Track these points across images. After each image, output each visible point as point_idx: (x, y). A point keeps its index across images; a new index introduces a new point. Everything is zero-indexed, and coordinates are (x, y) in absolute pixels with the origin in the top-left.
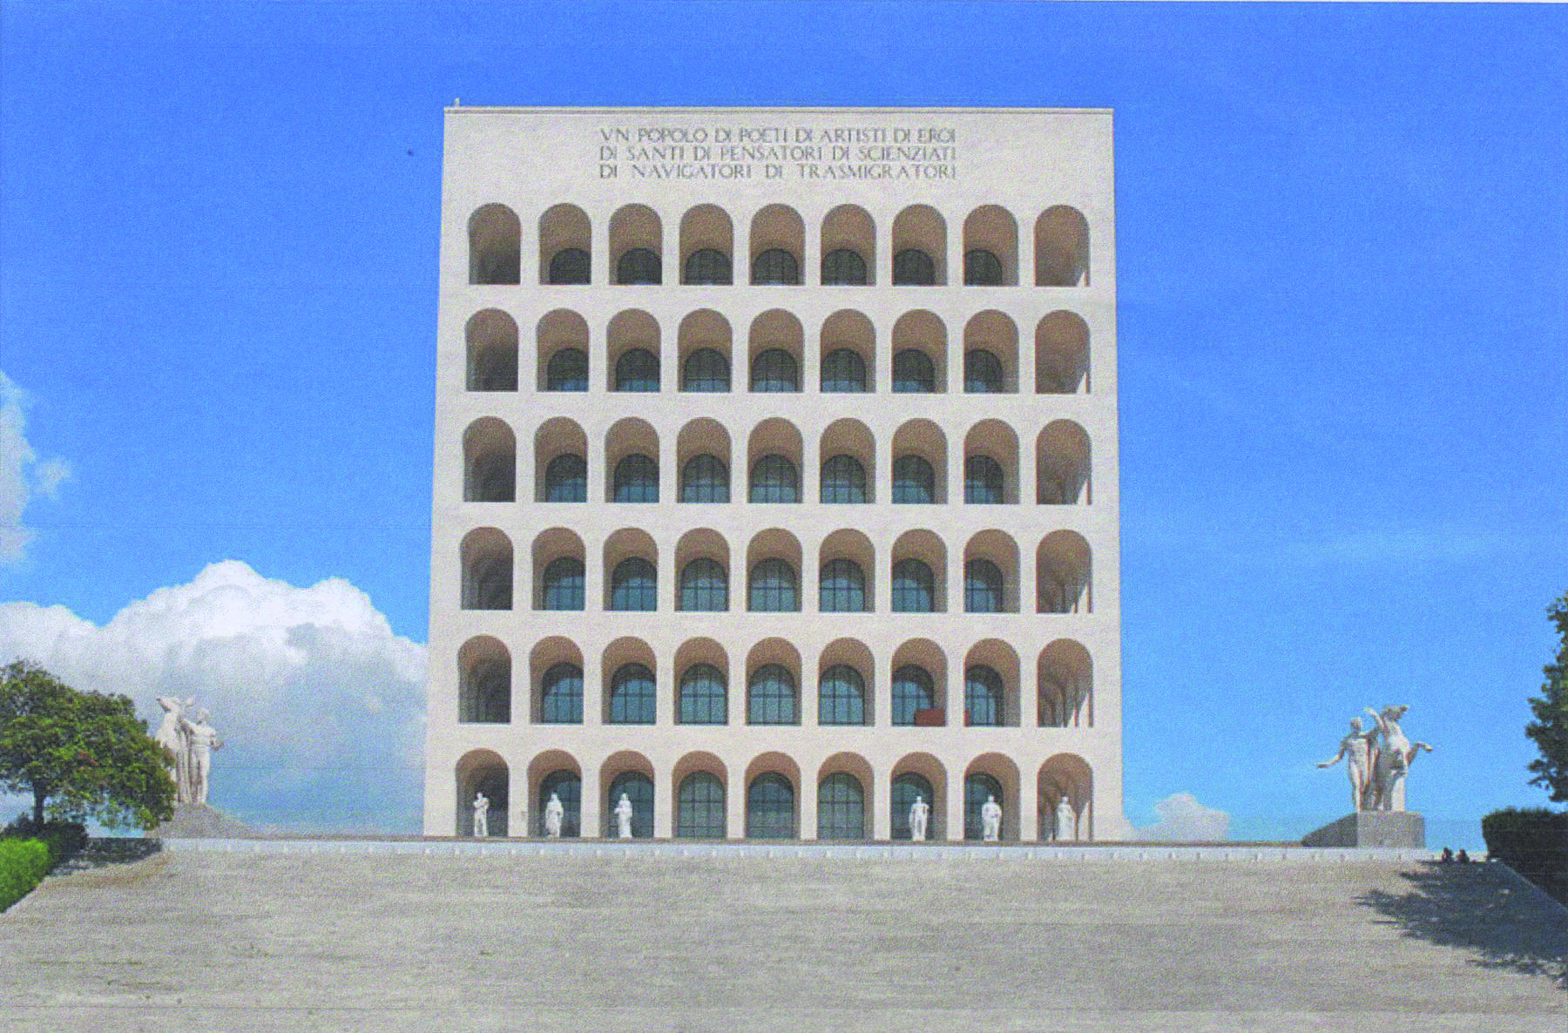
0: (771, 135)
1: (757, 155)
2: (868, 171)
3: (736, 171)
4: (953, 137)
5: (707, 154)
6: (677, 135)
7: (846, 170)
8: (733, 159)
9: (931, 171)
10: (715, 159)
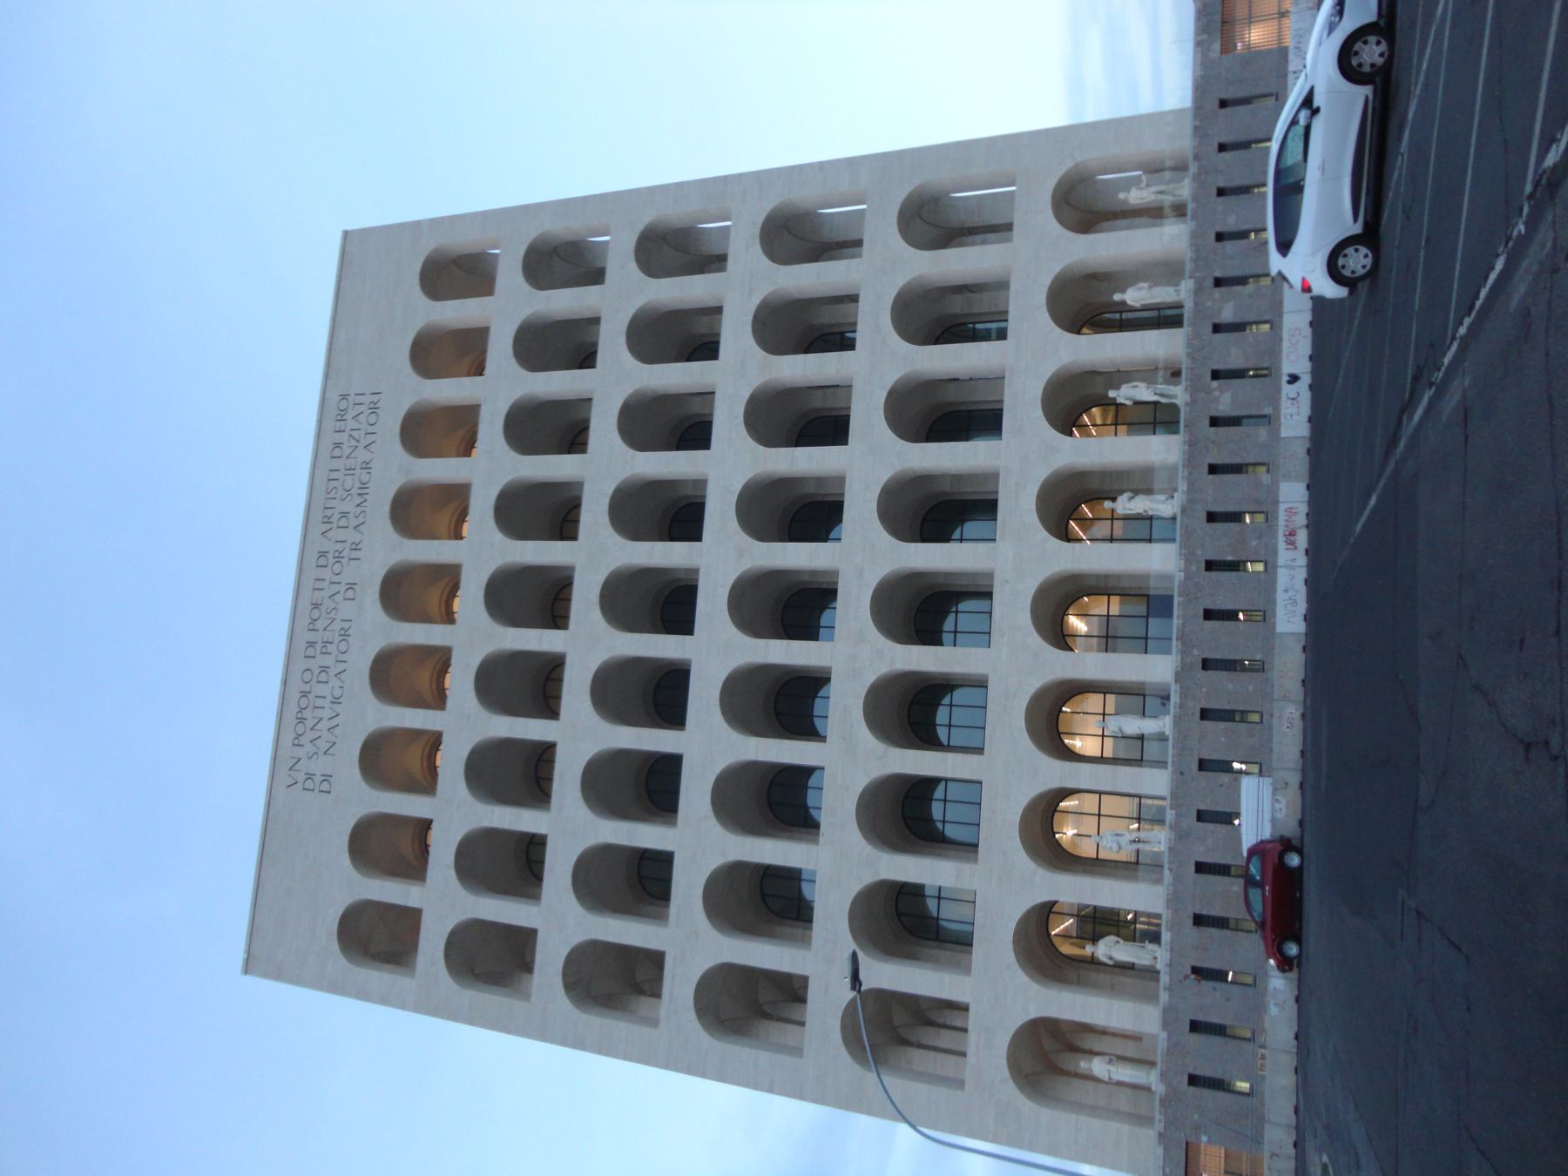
1: (332, 615)
3: (345, 635)
4: (344, 397)
5: (324, 669)
6: (304, 702)
7: (359, 510)
8: (331, 643)
9: (373, 419)
10: (328, 661)
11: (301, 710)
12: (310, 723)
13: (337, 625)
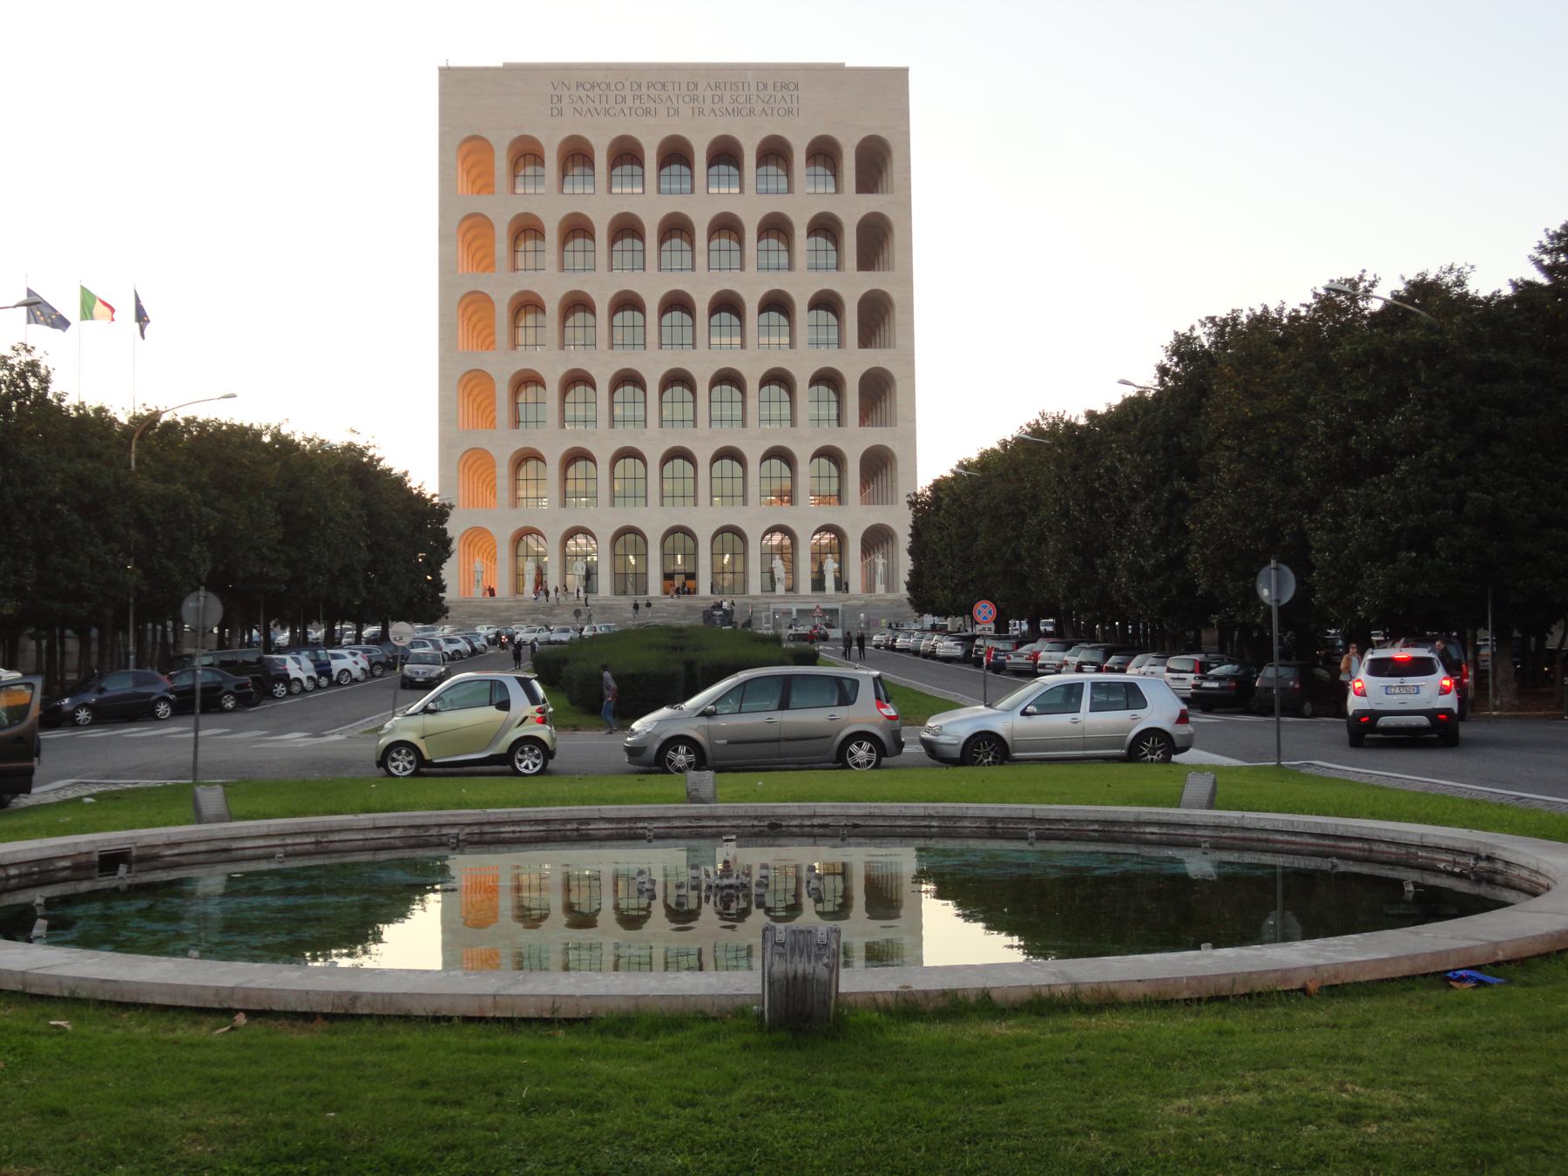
0: (670, 86)
2: (740, 112)
3: (647, 112)
4: (797, 87)
5: (624, 99)
6: (603, 86)
7: (724, 111)
12: (590, 94)
13: (652, 105)
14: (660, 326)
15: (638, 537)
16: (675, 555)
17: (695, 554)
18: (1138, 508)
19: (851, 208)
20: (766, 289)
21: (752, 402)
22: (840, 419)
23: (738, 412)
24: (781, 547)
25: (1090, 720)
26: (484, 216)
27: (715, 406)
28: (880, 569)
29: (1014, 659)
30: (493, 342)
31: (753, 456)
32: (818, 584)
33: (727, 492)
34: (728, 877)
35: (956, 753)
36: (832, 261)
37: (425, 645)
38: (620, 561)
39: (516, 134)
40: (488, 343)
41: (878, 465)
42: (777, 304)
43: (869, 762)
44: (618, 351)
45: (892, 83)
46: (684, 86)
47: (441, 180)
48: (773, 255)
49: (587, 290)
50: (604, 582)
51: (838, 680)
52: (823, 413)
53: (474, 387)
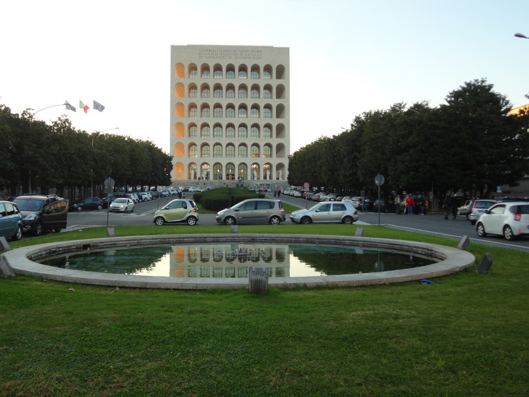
2: (247, 58)
3: (223, 58)
4: (261, 52)
5: (218, 54)
6: (212, 51)
11: (211, 50)
12: (209, 53)
13: (225, 56)
14: (226, 112)
15: (220, 165)
16: (229, 170)
17: (234, 170)
18: (345, 160)
19: (275, 83)
20: (253, 103)
21: (249, 132)
22: (271, 136)
23: (245, 134)
24: (256, 168)
25: (332, 213)
26: (182, 84)
27: (240, 132)
28: (281, 174)
29: (314, 197)
30: (184, 115)
31: (249, 145)
32: (265, 178)
33: (243, 154)
34: (241, 253)
35: (299, 221)
36: (270, 96)
37: (166, 192)
38: (215, 171)
39: (190, 63)
40: (182, 115)
41: (281, 148)
42: (256, 126)
43: (277, 223)
44: (215, 118)
45: (285, 51)
46: (233, 51)
47: (171, 74)
48: (255, 94)
49: (208, 102)
50: (211, 176)
51: (270, 202)
52: (267, 134)
53: (179, 127)
